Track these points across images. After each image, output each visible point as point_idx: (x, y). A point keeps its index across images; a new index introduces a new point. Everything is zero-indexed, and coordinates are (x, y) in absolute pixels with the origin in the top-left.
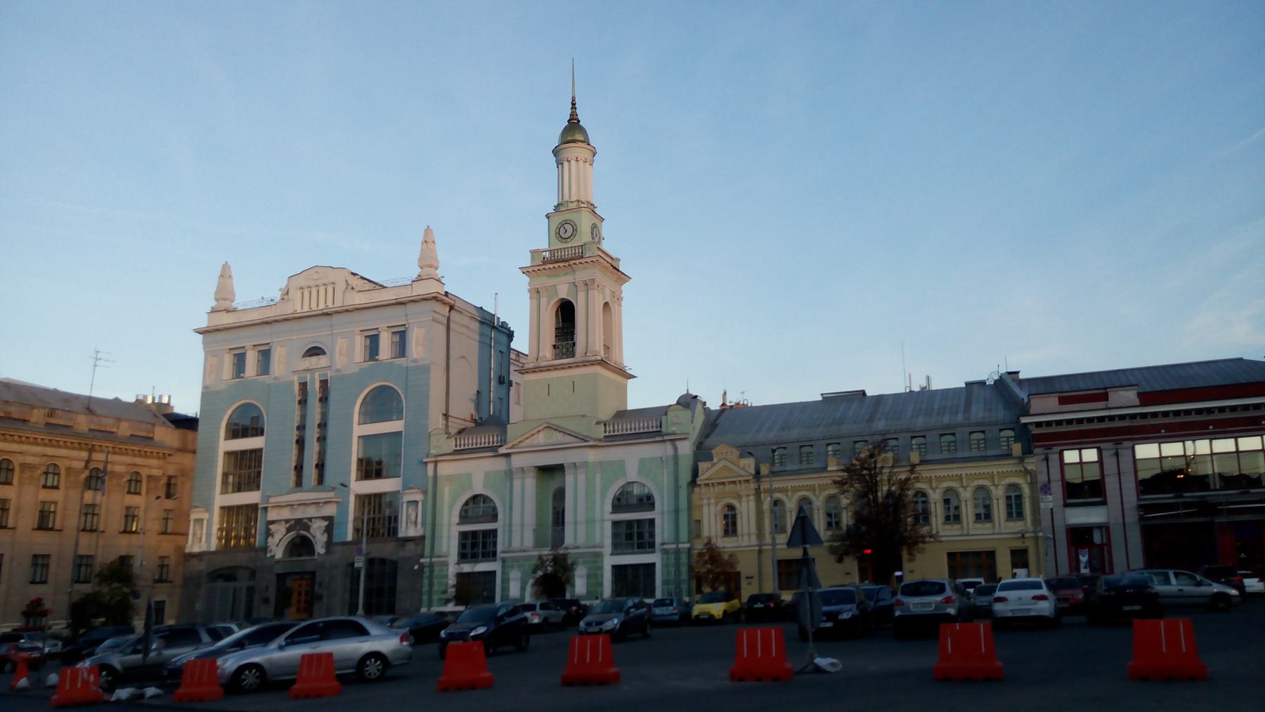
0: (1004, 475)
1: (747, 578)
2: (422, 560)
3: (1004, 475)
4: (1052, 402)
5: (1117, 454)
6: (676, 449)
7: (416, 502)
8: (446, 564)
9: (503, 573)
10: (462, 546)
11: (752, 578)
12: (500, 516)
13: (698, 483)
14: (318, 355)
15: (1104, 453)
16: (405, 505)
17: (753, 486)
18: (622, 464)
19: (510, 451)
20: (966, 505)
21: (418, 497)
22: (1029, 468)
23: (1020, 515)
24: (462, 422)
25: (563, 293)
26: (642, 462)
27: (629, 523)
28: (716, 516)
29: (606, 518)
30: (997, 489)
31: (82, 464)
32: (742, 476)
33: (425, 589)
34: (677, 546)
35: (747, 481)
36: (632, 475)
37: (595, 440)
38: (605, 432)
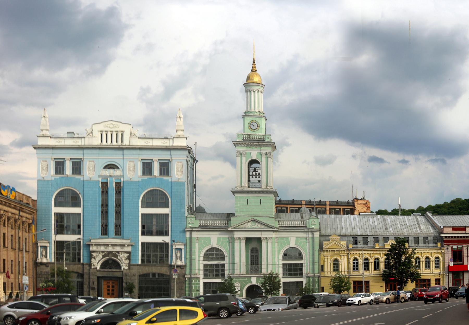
0: (434, 253)
6: (313, 235)
8: (198, 278)
10: (205, 270)
12: (226, 258)
14: (114, 168)
16: (174, 250)
21: (182, 247)
23: (439, 267)
25: (254, 156)
27: (290, 265)
33: (187, 289)
35: (344, 250)
37: (277, 228)
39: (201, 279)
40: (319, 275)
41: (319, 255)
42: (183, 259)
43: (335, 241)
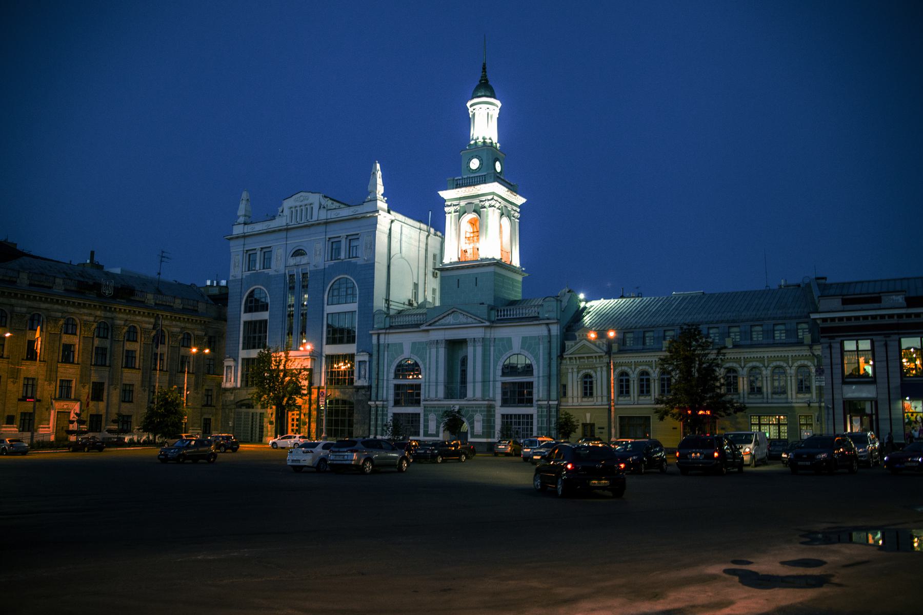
0: (795, 359)
1: (599, 428)
2: (369, 403)
3: (795, 359)
4: (836, 303)
5: (886, 345)
6: (549, 331)
7: (365, 362)
9: (425, 415)
11: (603, 428)
13: (564, 357)
15: (876, 344)
17: (606, 360)
18: (509, 340)
19: (429, 328)
20: (767, 380)
21: (366, 358)
22: (818, 353)
24: (402, 305)
26: (525, 340)
28: (577, 382)
29: (498, 380)
30: (766, 369)
31: (151, 326)
32: (597, 353)
34: (548, 403)
35: (600, 357)
36: (407, 353)
38: (498, 316)
39: (391, 408)
40: (556, 403)
41: (559, 365)
42: (367, 379)
43: (584, 340)
